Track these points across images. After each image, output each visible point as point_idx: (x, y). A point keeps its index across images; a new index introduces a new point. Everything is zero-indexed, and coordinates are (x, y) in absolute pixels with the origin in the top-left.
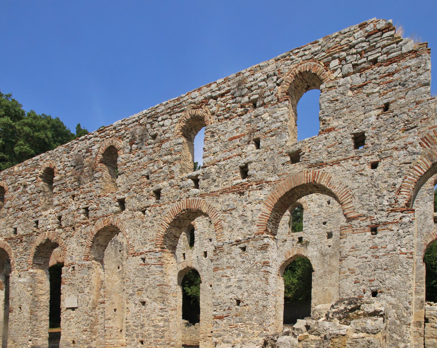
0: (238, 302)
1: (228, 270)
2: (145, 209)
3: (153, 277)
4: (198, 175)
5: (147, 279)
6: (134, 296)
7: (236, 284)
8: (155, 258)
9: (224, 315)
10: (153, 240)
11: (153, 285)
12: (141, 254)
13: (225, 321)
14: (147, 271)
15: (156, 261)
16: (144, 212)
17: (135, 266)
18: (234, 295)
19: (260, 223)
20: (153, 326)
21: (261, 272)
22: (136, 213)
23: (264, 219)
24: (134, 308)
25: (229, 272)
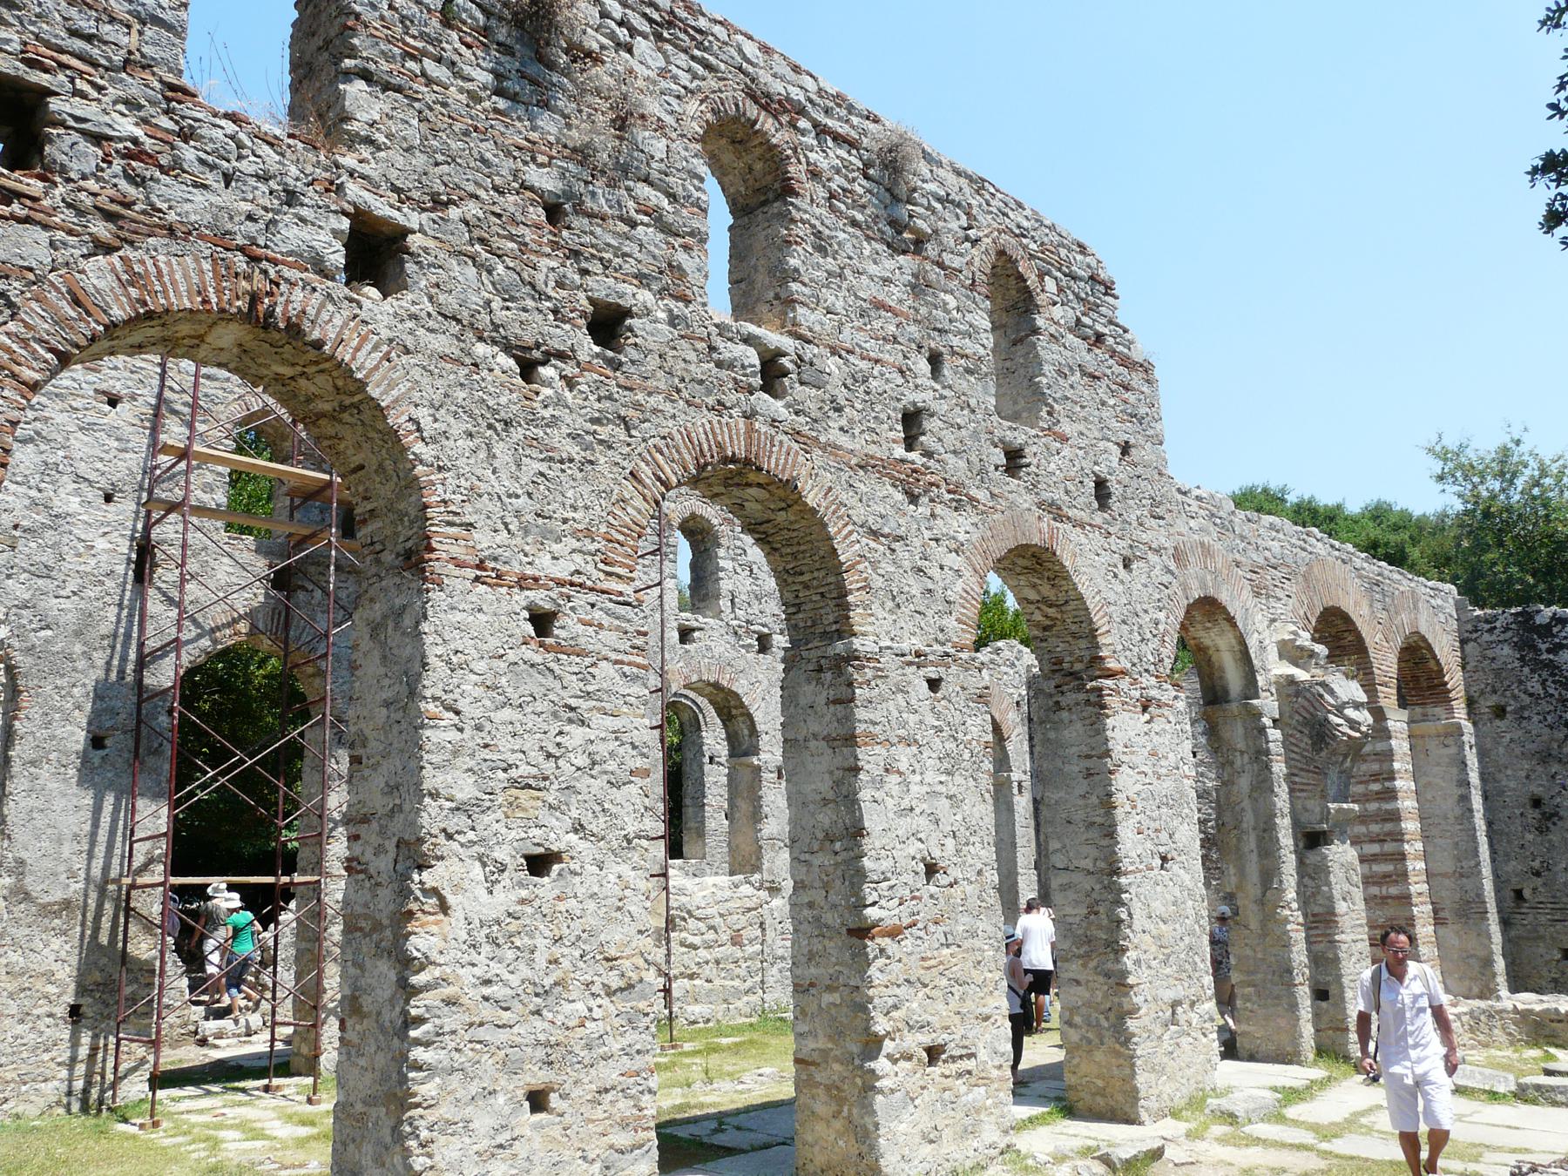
0: (931, 870)
1: (901, 747)
2: (536, 354)
3: (609, 722)
5: (577, 735)
6: (487, 819)
7: (925, 806)
8: (618, 628)
9: (906, 921)
10: (589, 534)
11: (612, 766)
12: (523, 583)
13: (908, 943)
14: (575, 685)
15: (626, 646)
17: (493, 643)
20: (610, 993)
22: (481, 349)
24: (481, 892)
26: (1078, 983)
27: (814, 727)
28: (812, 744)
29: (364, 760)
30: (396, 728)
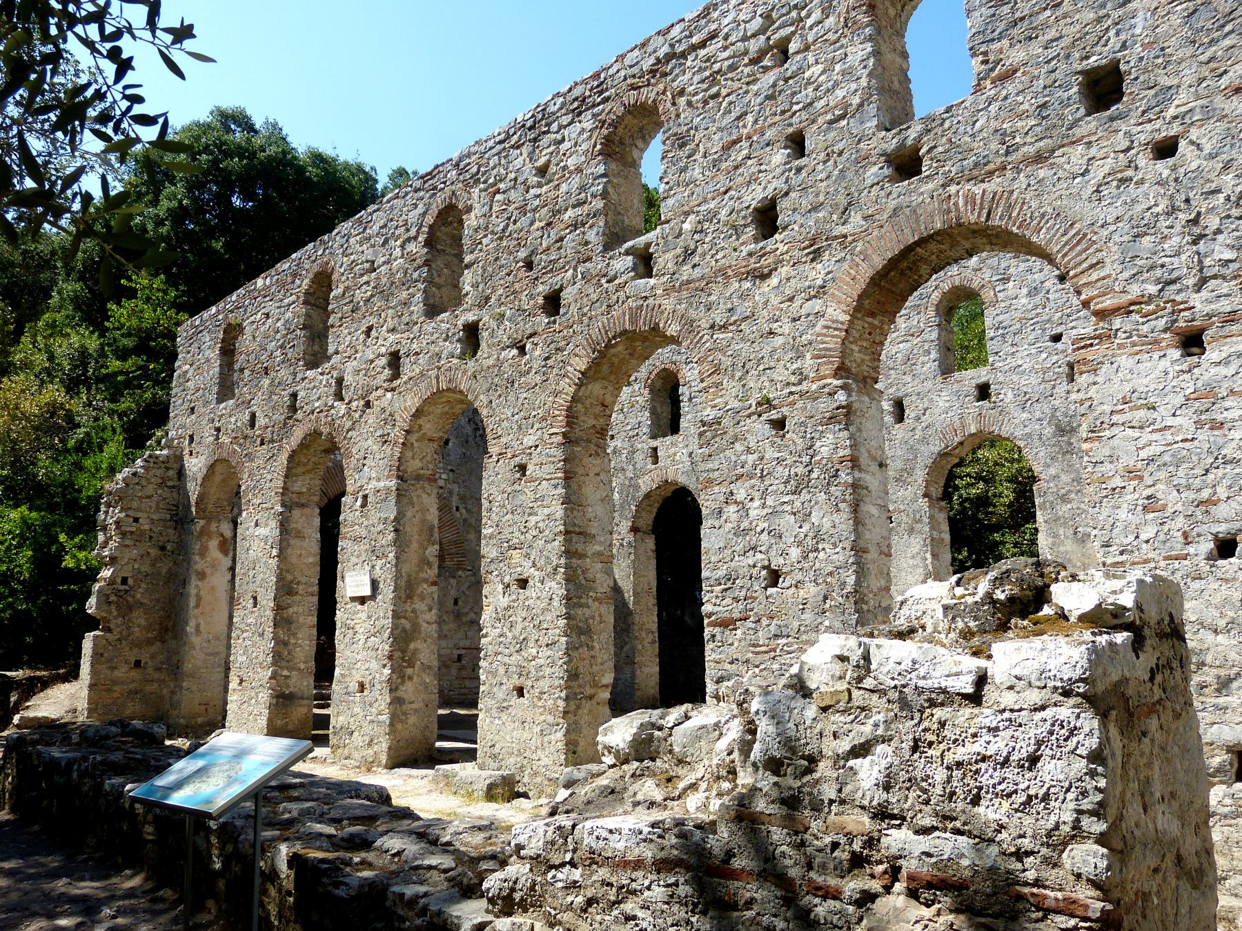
3: (547, 511)
4: (648, 245)
5: (533, 519)
14: (531, 495)
16: (522, 350)
18: (759, 556)
19: (820, 350)
21: (833, 488)
23: (833, 336)
25: (742, 491)
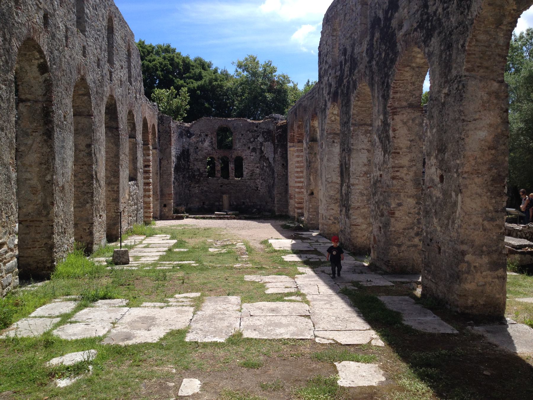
26: (333, 209)
27: (364, 147)
28: (362, 151)
29: (401, 153)
30: (413, 147)
